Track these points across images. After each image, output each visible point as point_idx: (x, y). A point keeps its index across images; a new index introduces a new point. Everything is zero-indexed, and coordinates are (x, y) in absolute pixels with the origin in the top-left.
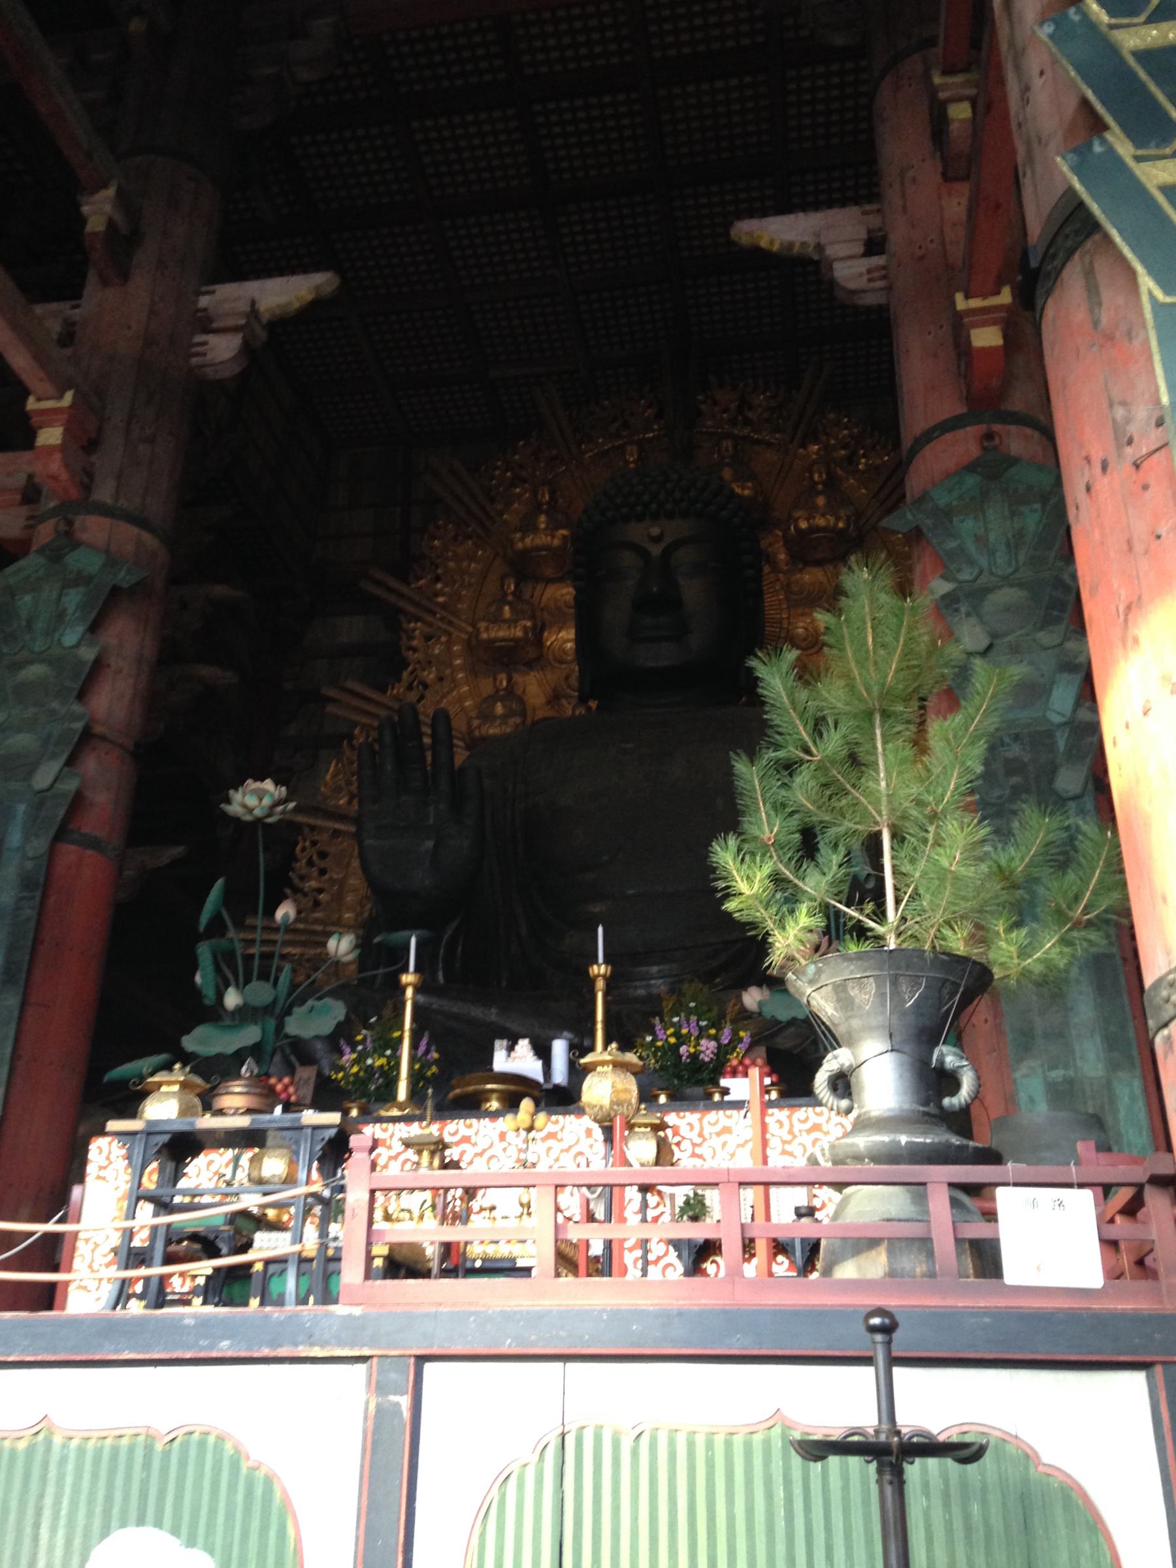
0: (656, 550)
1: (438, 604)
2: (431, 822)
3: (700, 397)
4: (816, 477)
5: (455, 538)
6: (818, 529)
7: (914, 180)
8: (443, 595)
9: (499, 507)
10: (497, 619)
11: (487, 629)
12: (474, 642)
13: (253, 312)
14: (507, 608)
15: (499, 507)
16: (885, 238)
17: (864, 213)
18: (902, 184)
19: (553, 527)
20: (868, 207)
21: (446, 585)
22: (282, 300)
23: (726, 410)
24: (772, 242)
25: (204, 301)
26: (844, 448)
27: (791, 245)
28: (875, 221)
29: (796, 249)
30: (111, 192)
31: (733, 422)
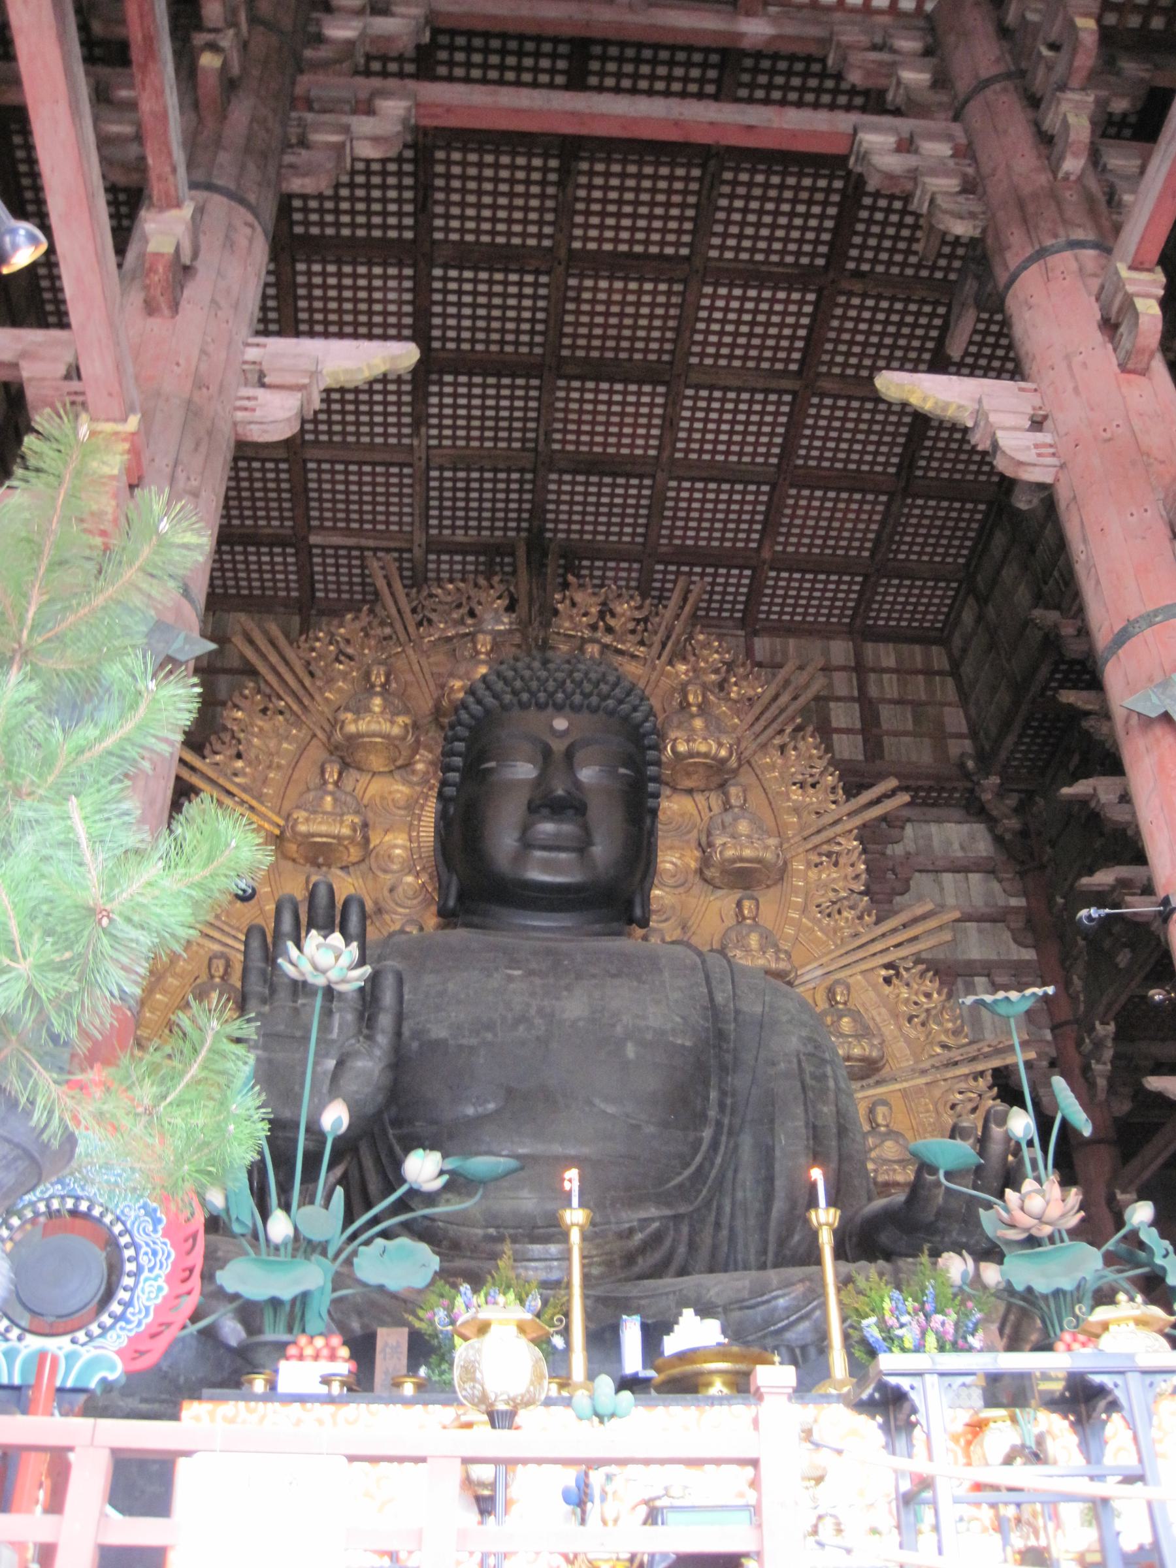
0: (558, 746)
1: (238, 785)
2: (334, 1035)
3: (557, 596)
4: (691, 698)
5: (264, 711)
6: (699, 754)
7: (1085, 365)
8: (245, 775)
9: (319, 683)
10: (315, 810)
11: (307, 820)
12: (288, 834)
13: (314, 374)
14: (329, 799)
15: (319, 683)
16: (1045, 417)
17: (1022, 390)
18: (1070, 367)
19: (391, 711)
20: (1022, 384)
21: (249, 763)
22: (349, 364)
23: (585, 614)
24: (925, 399)
25: (252, 354)
26: (716, 671)
27: (947, 405)
28: (1036, 400)
29: (950, 413)
30: (187, 211)
31: (594, 627)
